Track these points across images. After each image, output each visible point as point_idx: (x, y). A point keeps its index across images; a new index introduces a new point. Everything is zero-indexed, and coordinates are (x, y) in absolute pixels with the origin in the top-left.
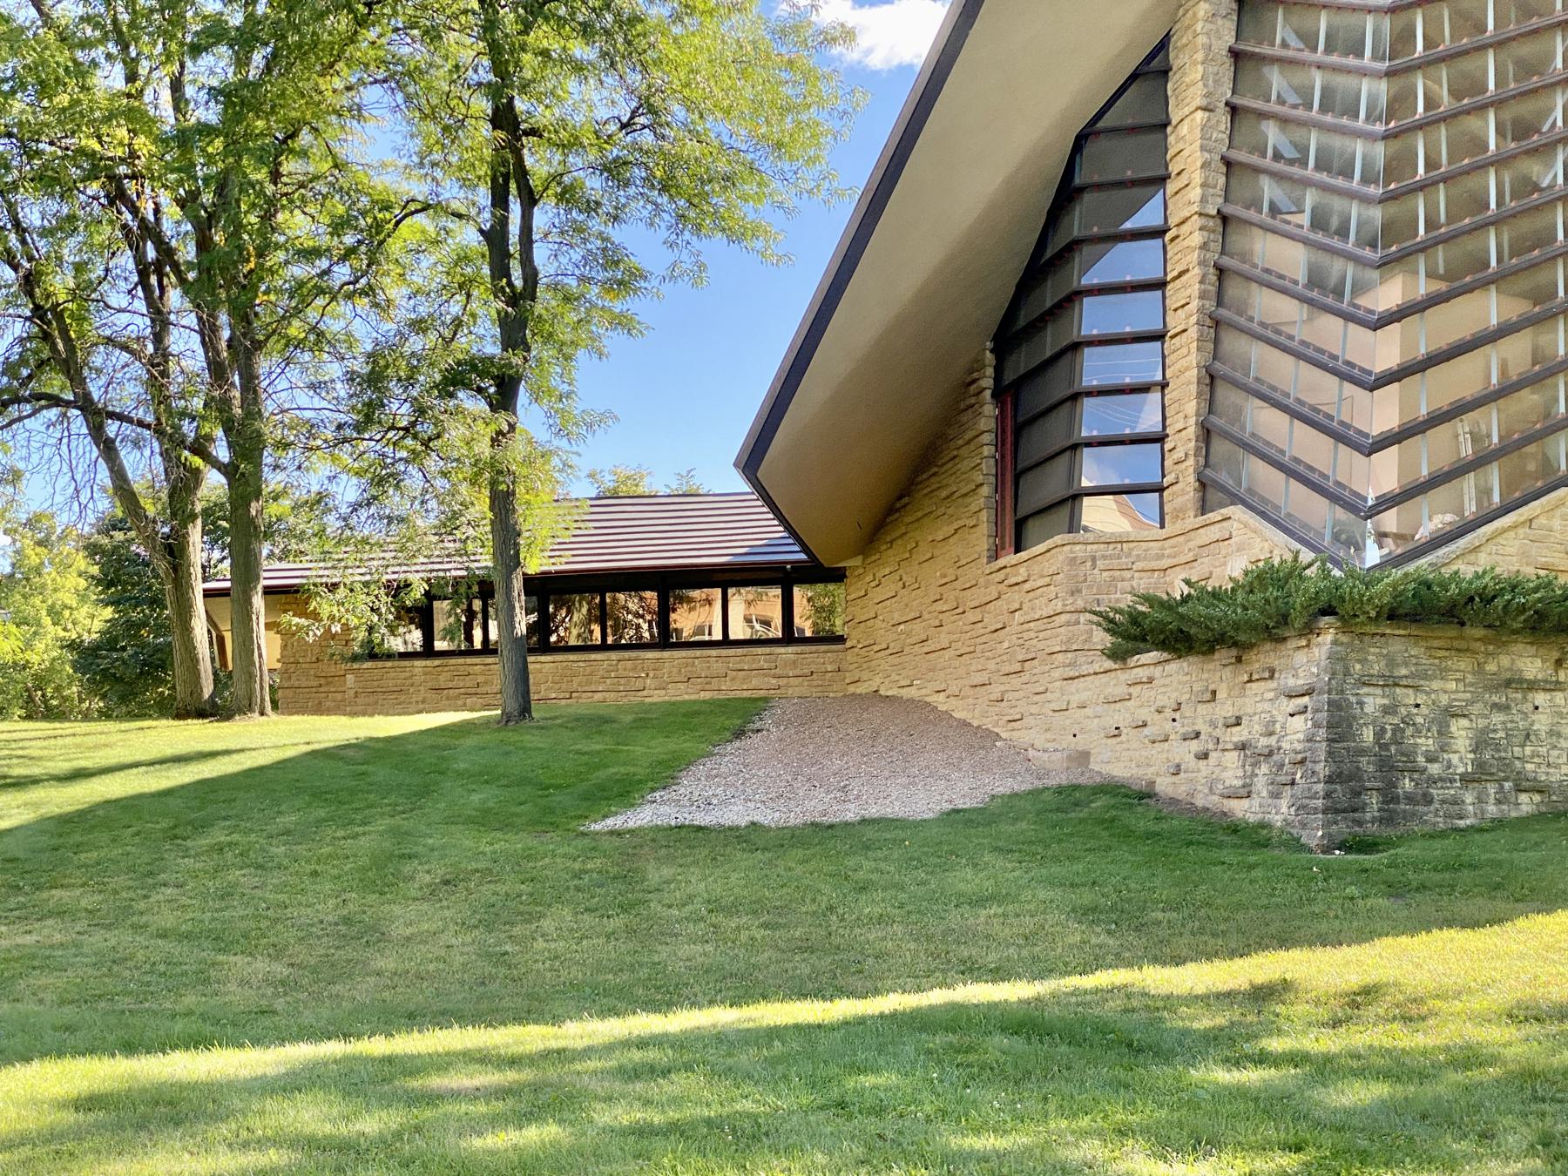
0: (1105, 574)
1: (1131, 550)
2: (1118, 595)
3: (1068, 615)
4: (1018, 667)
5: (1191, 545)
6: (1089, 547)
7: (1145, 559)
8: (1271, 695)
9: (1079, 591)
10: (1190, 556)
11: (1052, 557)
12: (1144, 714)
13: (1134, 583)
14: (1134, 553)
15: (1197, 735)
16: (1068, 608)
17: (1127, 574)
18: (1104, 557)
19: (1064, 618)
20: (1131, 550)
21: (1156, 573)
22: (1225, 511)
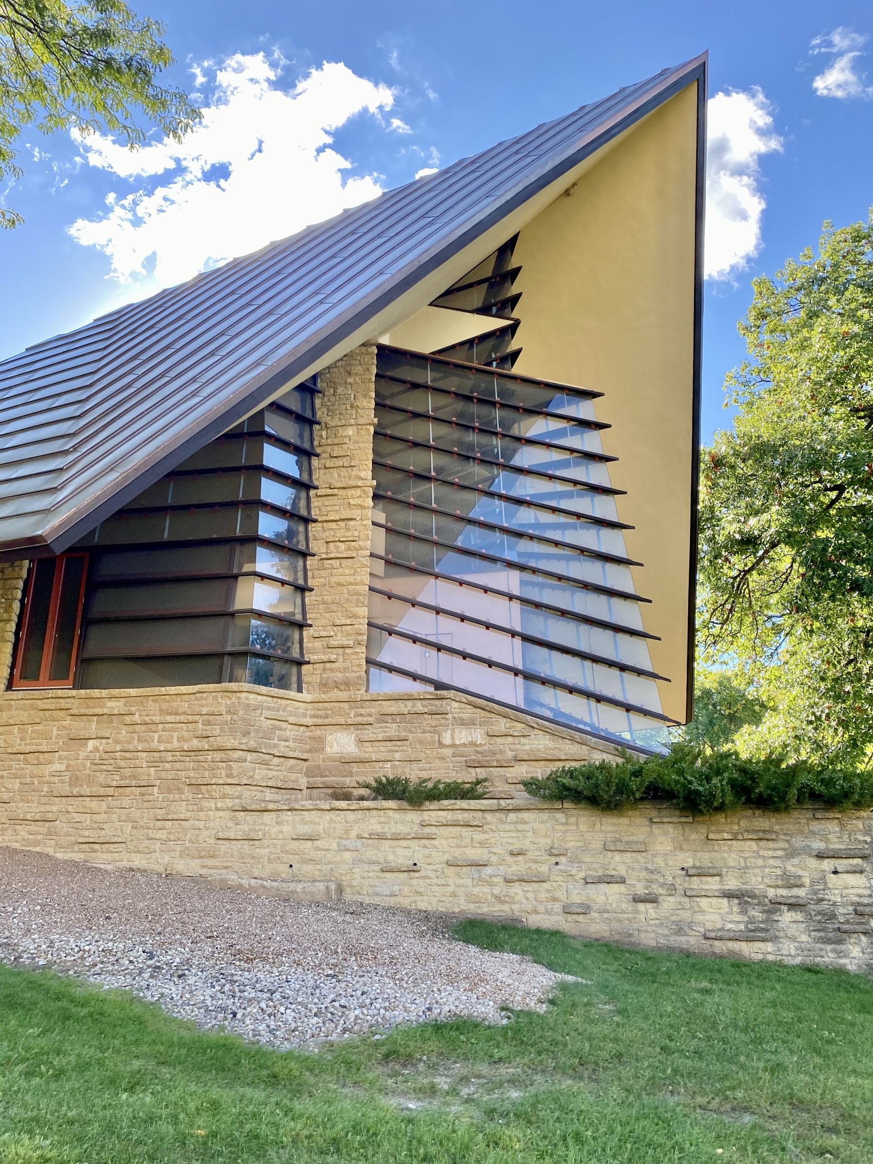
0: (269, 722)
1: (287, 706)
2: (276, 741)
3: (241, 752)
4: (110, 791)
5: (362, 711)
6: (260, 697)
7: (296, 716)
8: (780, 853)
9: (249, 733)
10: (370, 720)
11: (202, 698)
12: (474, 854)
13: (288, 733)
14: (289, 709)
15: (623, 881)
16: (243, 747)
17: (284, 725)
18: (269, 708)
19: (237, 755)
20: (287, 706)
21: (302, 728)
22: (444, 693)
